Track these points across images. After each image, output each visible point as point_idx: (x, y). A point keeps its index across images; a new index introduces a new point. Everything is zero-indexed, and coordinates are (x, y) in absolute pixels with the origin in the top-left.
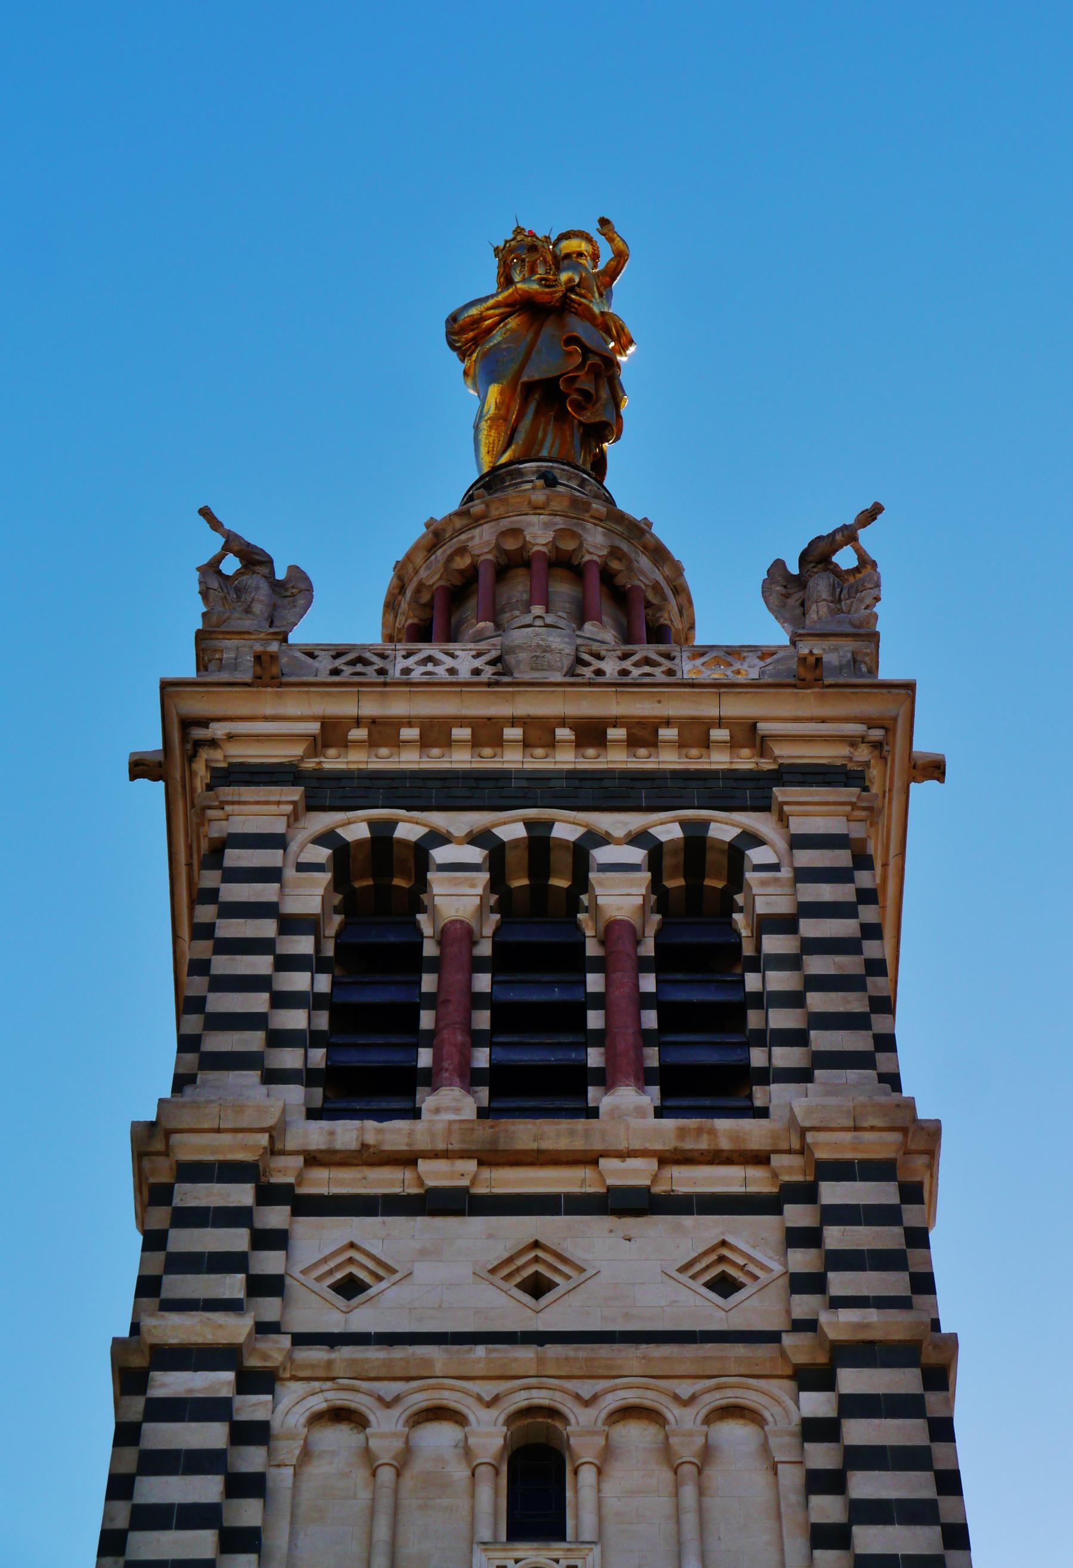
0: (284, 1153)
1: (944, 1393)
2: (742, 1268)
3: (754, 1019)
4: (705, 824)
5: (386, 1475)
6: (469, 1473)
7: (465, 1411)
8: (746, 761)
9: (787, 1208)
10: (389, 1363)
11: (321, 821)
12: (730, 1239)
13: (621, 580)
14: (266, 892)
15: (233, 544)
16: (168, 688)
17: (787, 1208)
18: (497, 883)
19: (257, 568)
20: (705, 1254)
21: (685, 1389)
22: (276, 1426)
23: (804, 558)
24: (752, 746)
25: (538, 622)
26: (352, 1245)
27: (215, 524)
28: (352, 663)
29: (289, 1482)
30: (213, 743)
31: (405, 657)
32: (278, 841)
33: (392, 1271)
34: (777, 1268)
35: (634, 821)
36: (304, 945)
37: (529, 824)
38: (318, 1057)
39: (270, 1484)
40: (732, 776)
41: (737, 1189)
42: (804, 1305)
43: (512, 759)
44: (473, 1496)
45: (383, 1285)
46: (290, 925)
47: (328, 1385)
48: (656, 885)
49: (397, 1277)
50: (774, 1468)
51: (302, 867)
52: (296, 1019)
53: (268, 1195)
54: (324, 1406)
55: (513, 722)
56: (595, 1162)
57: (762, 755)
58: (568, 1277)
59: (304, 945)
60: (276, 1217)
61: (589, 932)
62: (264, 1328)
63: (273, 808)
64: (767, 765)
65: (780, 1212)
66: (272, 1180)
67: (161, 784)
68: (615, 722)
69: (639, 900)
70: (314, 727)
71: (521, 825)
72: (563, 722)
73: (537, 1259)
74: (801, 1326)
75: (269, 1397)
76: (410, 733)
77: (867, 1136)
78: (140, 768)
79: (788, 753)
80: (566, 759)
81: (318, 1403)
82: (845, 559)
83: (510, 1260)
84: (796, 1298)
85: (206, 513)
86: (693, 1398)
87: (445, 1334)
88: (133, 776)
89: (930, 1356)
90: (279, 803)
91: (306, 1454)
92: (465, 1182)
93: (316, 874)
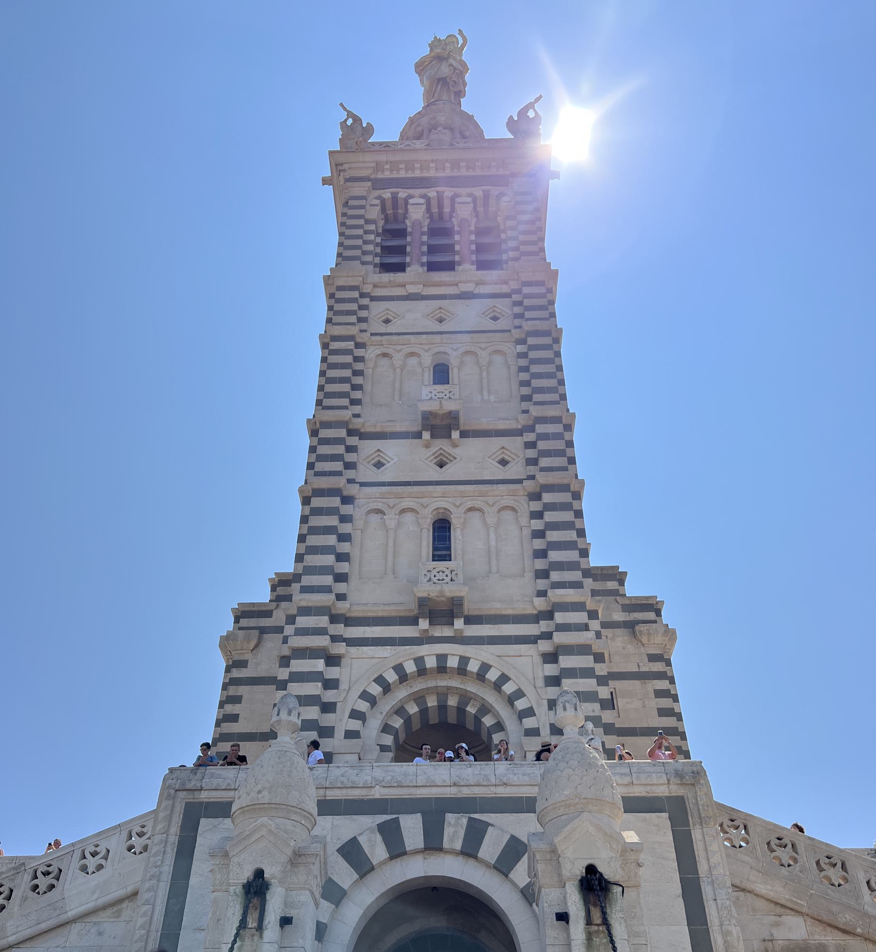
0: (367, 283)
1: (558, 344)
2: (500, 313)
3: (504, 246)
4: (489, 191)
5: (398, 371)
6: (422, 370)
7: (421, 353)
11: (377, 193)
12: (496, 305)
14: (361, 212)
15: (350, 114)
16: (331, 153)
18: (428, 209)
19: (357, 122)
20: (489, 309)
21: (483, 346)
22: (366, 357)
23: (519, 114)
25: (439, 132)
26: (387, 309)
27: (345, 109)
28: (385, 147)
29: (371, 372)
30: (344, 170)
31: (400, 145)
32: (364, 198)
33: (399, 316)
34: (510, 312)
35: (468, 190)
36: (372, 227)
38: (377, 260)
39: (365, 373)
42: (517, 322)
44: (423, 376)
45: (396, 320)
46: (368, 222)
47: (381, 347)
48: (475, 208)
49: (399, 318)
50: (509, 367)
51: (371, 205)
52: (370, 247)
53: (362, 295)
54: (380, 352)
58: (450, 317)
59: (372, 227)
60: (365, 301)
61: (455, 224)
62: (362, 331)
63: (363, 189)
66: (364, 291)
67: (332, 186)
69: (470, 212)
70: (374, 165)
73: (440, 312)
74: (516, 327)
75: (364, 350)
76: (402, 166)
78: (325, 181)
81: (378, 352)
82: (531, 114)
83: (432, 312)
84: (516, 320)
85: (341, 105)
86: (486, 348)
87: (414, 333)
89: (554, 335)
90: (364, 187)
91: (376, 366)
92: (419, 291)
93: (376, 207)
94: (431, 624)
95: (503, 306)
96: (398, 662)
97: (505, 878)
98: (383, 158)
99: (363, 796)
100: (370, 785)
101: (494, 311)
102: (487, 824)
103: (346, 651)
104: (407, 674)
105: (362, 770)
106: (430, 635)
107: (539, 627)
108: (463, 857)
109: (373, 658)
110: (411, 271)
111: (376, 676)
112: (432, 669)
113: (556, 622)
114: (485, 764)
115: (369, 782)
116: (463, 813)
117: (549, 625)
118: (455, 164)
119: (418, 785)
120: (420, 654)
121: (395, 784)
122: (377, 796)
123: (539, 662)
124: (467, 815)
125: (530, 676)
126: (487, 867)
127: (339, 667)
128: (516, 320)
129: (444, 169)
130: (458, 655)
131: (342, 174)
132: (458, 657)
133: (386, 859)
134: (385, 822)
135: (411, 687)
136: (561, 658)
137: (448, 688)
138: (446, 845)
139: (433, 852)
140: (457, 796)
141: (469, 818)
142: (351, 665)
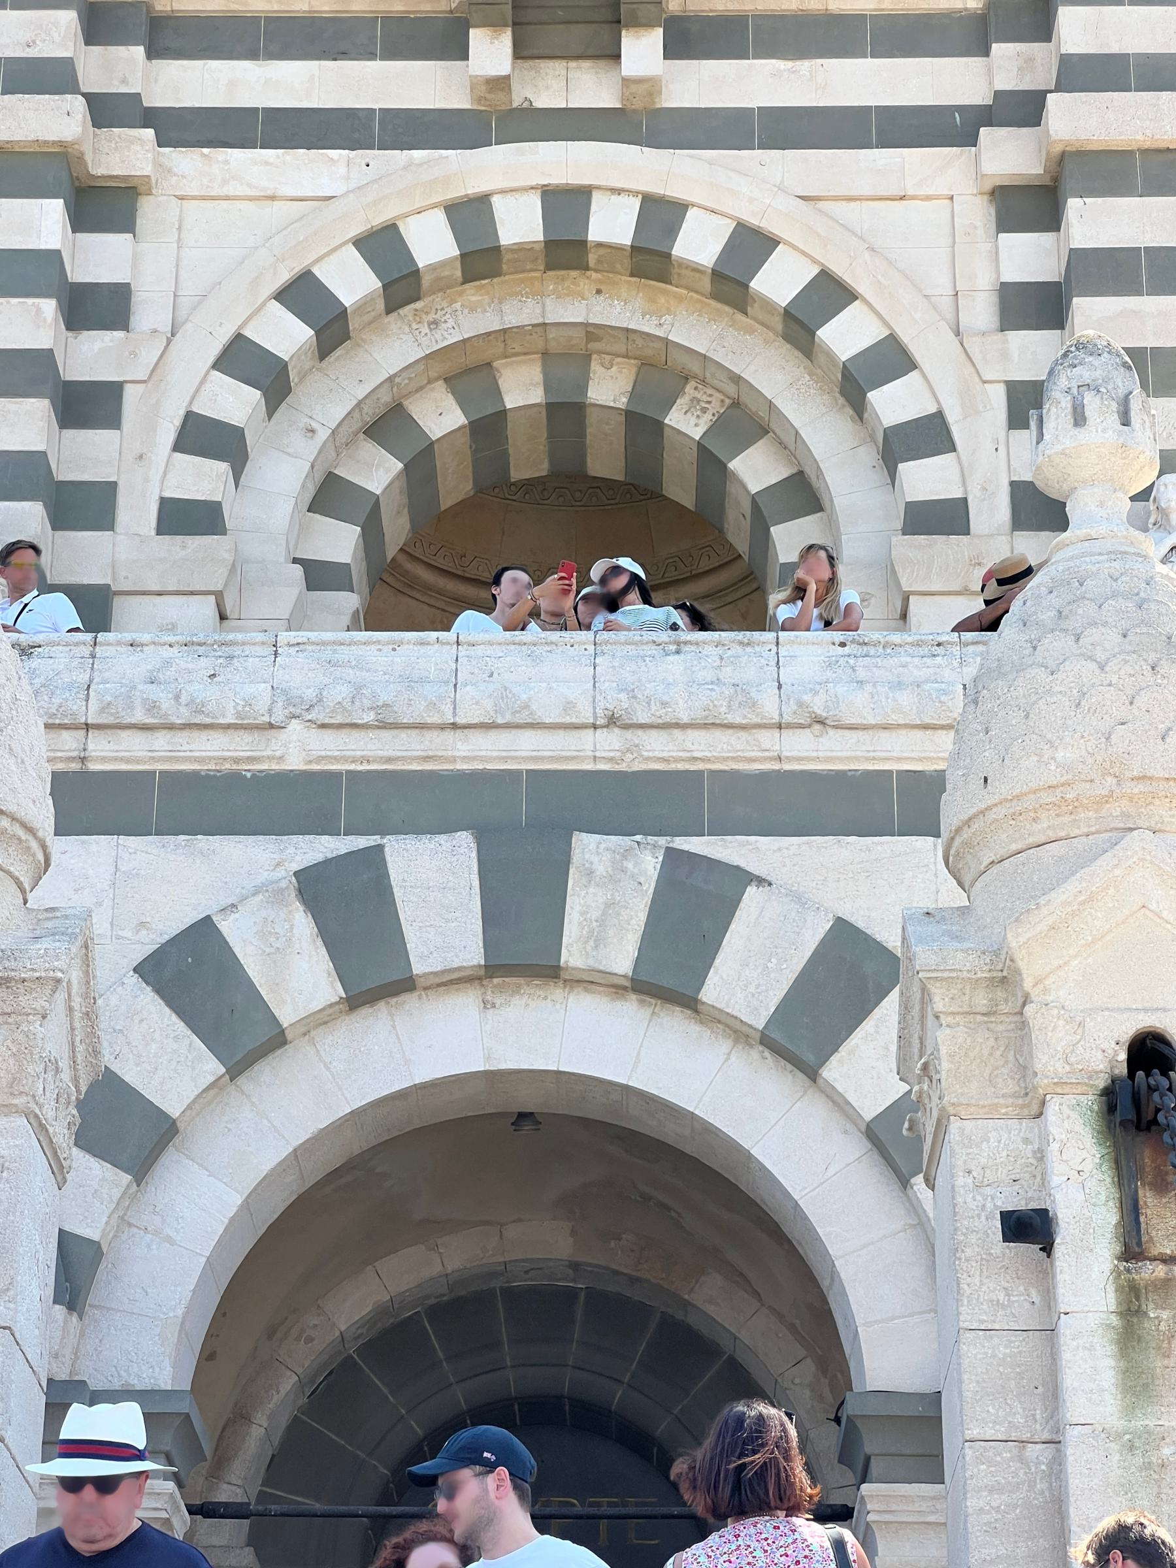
94: (521, 52)
96: (379, 219)
97: (808, 1082)
99: (237, 760)
100: (266, 719)
102: (743, 878)
103: (158, 165)
104: (418, 270)
105: (231, 657)
106: (515, 105)
107: (989, 70)
108: (641, 1002)
109: (273, 198)
111: (284, 276)
112: (520, 249)
113: (1063, 51)
114: (741, 643)
115: (262, 705)
116: (646, 834)
117: (1030, 60)
119: (461, 720)
120: (474, 188)
121: (369, 717)
122: (295, 762)
123: (979, 224)
124: (662, 841)
125: (941, 285)
126: (736, 1041)
127: (129, 236)
130: (635, 193)
132: (636, 203)
133: (331, 1005)
134: (327, 862)
135: (435, 323)
136: (1074, 206)
137: (592, 332)
138: (572, 955)
139: (521, 980)
140: (623, 767)
141: (670, 852)
142: (179, 229)
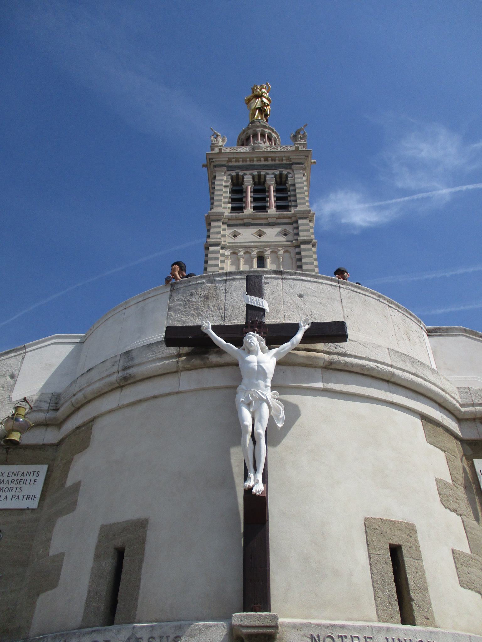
2: (288, 232)
3: (289, 199)
4: (282, 171)
8: (288, 162)
9: (294, 224)
10: (241, 246)
12: (286, 229)
13: (270, 137)
17: (294, 224)
18: (254, 180)
24: (289, 160)
28: (233, 149)
30: (213, 162)
34: (292, 232)
37: (258, 172)
38: (229, 205)
40: (287, 165)
41: (287, 222)
43: (255, 163)
49: (241, 234)
55: (255, 157)
56: (268, 219)
57: (290, 161)
64: (291, 162)
65: (293, 225)
67: (207, 168)
68: (270, 157)
70: (227, 159)
71: (257, 172)
72: (262, 157)
77: (305, 214)
78: (203, 166)
79: (293, 161)
80: (263, 162)
88: (203, 167)
92: (250, 222)
95: (289, 228)
98: (232, 156)
101: (285, 231)
110: (246, 212)
118: (266, 159)
128: (295, 236)
129: (261, 161)
131: (212, 163)
